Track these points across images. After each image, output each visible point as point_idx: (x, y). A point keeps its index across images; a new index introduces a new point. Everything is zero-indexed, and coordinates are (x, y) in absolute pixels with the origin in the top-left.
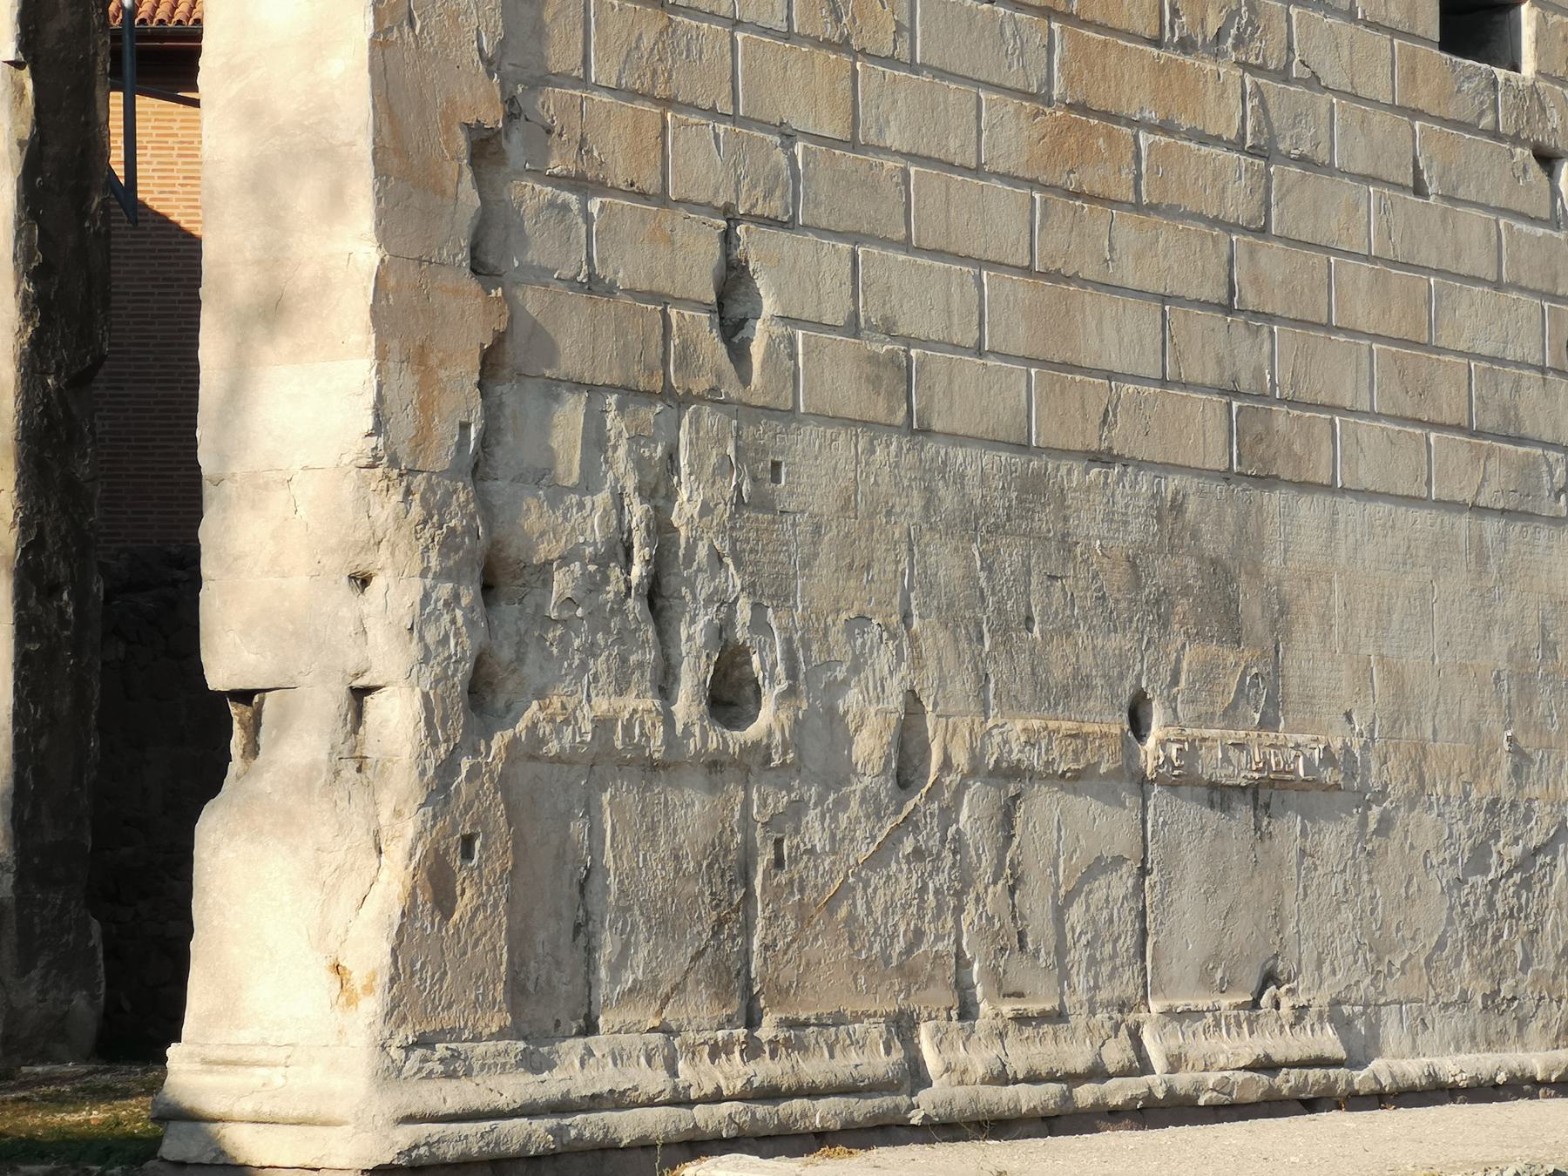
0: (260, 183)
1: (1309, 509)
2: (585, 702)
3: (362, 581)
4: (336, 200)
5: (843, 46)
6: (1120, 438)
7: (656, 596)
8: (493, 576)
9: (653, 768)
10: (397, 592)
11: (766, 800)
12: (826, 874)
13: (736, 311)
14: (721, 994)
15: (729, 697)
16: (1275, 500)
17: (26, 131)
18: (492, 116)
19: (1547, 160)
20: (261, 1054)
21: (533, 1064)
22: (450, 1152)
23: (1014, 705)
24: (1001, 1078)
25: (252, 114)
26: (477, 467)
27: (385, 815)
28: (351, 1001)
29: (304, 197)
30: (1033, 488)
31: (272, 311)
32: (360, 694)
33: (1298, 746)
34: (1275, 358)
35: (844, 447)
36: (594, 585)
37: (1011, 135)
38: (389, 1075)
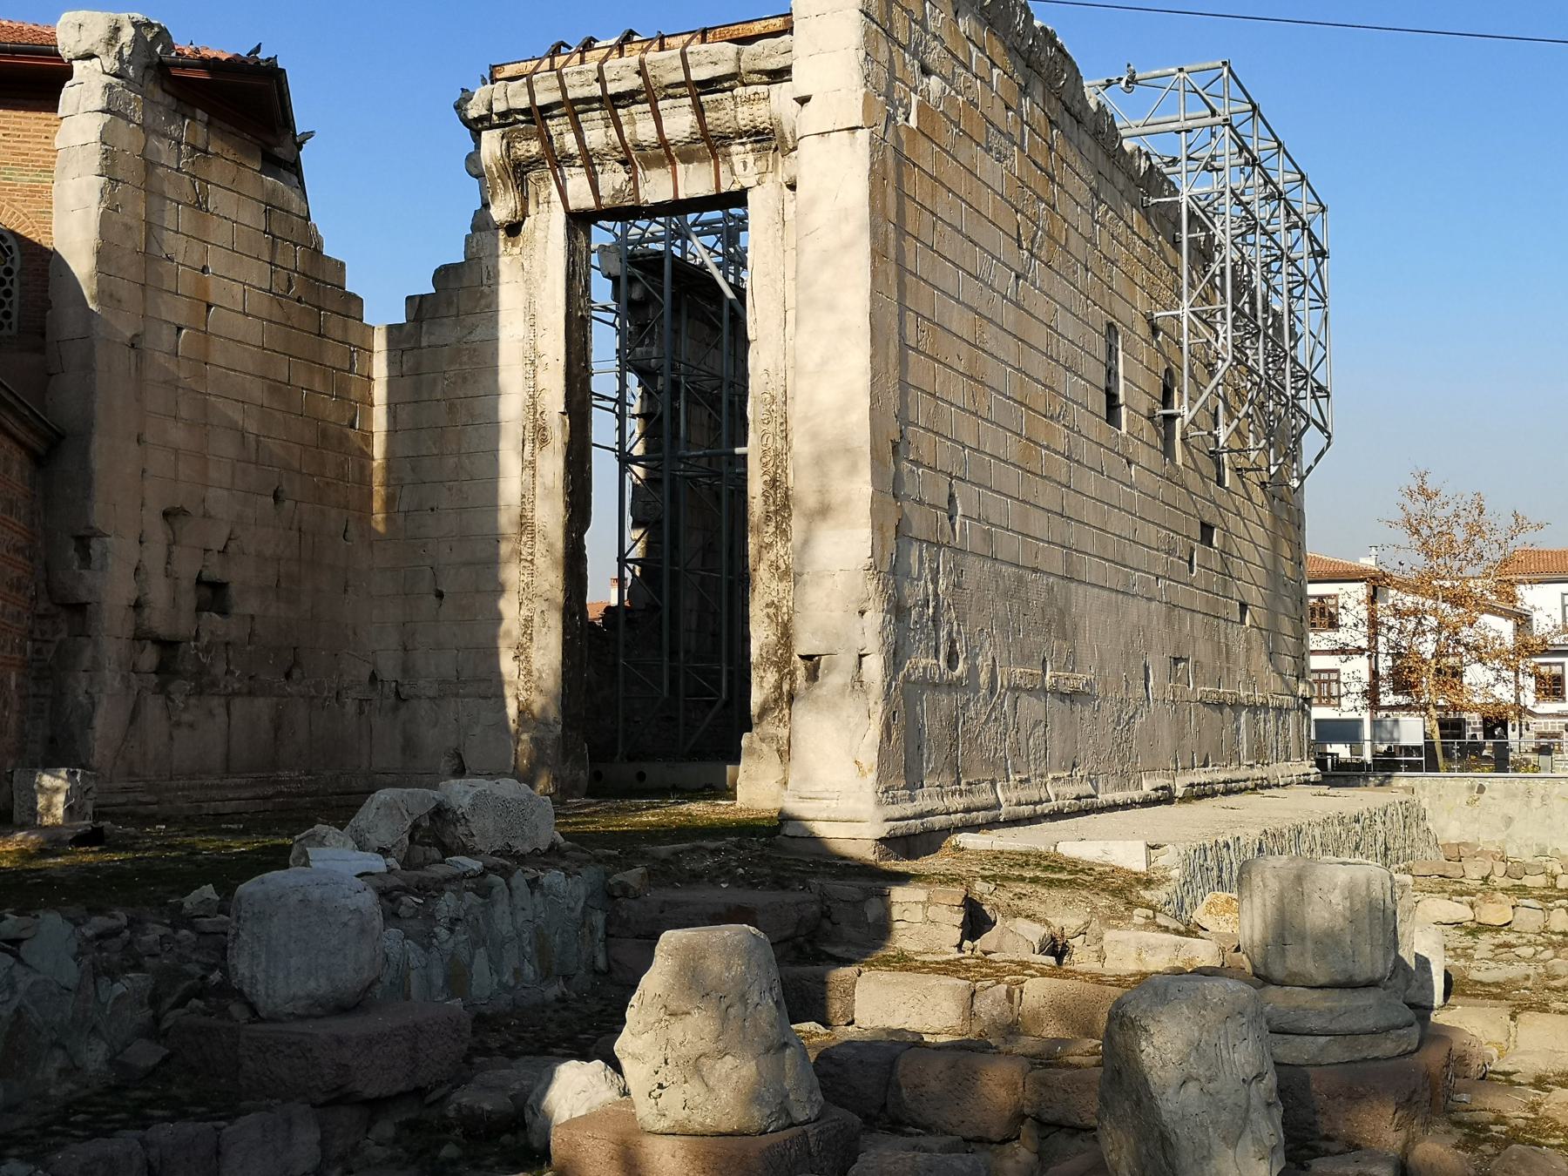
0: (819, 461)
1: (1081, 589)
2: (921, 662)
3: (862, 613)
4: (853, 470)
5: (975, 414)
6: (1040, 563)
7: (935, 619)
8: (898, 610)
9: (936, 685)
10: (875, 618)
11: (960, 698)
12: (975, 726)
14: (952, 774)
15: (952, 661)
16: (1073, 586)
17: (567, 439)
19: (1129, 463)
20: (826, 795)
21: (912, 799)
22: (899, 833)
23: (1018, 664)
24: (1019, 804)
25: (814, 436)
26: (894, 571)
27: (871, 704)
28: (864, 775)
29: (837, 468)
30: (1020, 579)
31: (823, 511)
32: (861, 656)
33: (1079, 680)
34: (1072, 534)
35: (978, 563)
36: (921, 616)
37: (1012, 448)
38: (879, 803)
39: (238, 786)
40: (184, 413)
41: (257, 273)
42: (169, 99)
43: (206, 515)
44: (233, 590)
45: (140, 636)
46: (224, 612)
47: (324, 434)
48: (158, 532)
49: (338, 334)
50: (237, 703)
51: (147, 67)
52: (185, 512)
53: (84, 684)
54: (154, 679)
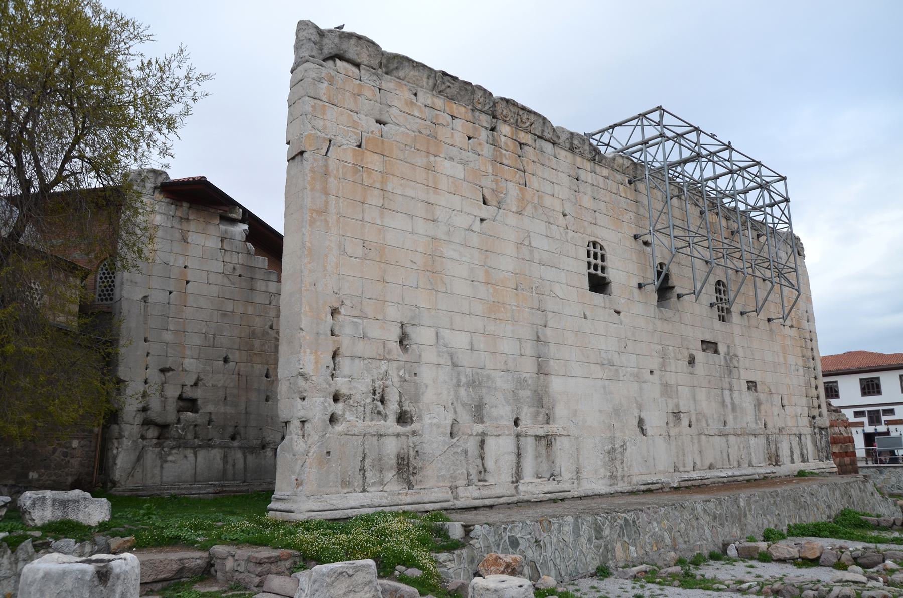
3: (303, 399)
13: (405, 343)
18: (336, 305)
32: (303, 422)
39: (199, 488)
40: (171, 327)
41: (219, 267)
42: (167, 200)
43: (184, 370)
44: (199, 402)
45: (147, 423)
46: (196, 412)
47: (254, 332)
48: (155, 377)
49: (263, 289)
50: (202, 453)
51: (155, 188)
52: (172, 370)
53: (116, 445)
54: (154, 441)
